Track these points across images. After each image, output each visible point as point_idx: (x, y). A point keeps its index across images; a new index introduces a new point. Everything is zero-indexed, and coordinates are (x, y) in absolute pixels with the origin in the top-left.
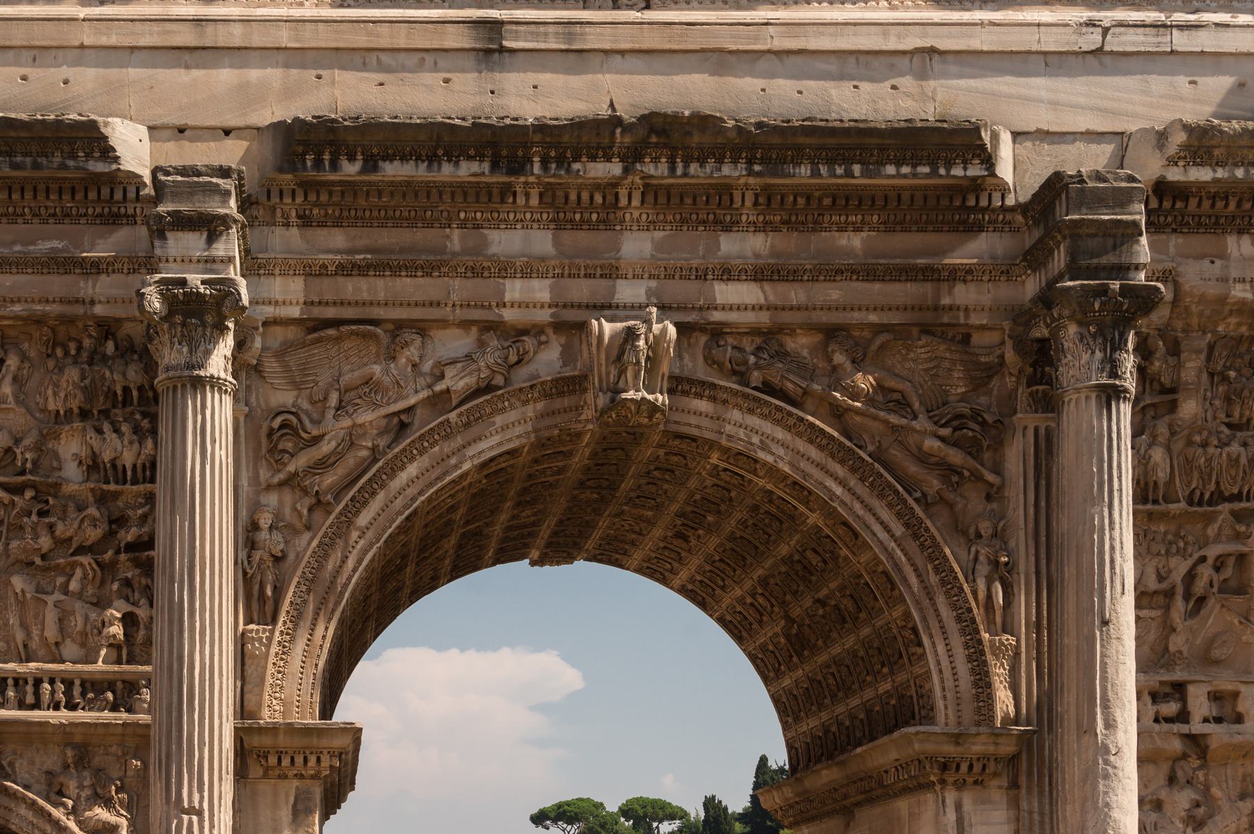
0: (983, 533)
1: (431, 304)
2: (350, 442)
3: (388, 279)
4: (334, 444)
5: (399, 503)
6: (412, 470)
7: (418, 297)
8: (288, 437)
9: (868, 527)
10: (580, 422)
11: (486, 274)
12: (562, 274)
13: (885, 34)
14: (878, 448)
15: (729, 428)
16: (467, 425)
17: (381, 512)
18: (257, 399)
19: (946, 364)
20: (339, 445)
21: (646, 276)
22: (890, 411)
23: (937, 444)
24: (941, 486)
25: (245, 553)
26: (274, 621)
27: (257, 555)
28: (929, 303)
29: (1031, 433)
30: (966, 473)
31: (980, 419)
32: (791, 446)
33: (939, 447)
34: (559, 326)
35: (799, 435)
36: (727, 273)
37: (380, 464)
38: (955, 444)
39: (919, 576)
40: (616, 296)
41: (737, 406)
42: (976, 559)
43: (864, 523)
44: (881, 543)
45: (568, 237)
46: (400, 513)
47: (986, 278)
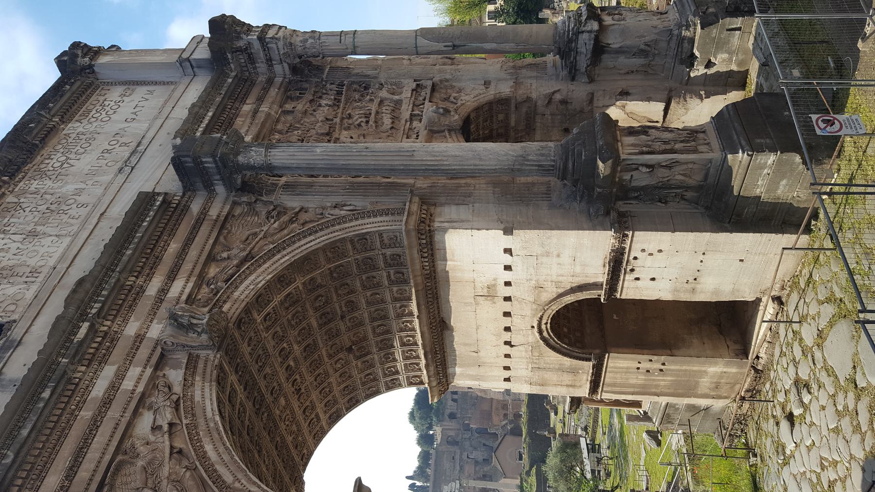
0: (321, 212)
3: (89, 451)
5: (226, 457)
6: (209, 448)
11: (112, 397)
12: (130, 360)
13: (85, 229)
15: (242, 297)
16: (193, 415)
19: (243, 222)
21: (150, 324)
34: (158, 367)
35: (255, 270)
36: (164, 291)
41: (232, 293)
42: (332, 215)
45: (112, 359)
46: (233, 456)
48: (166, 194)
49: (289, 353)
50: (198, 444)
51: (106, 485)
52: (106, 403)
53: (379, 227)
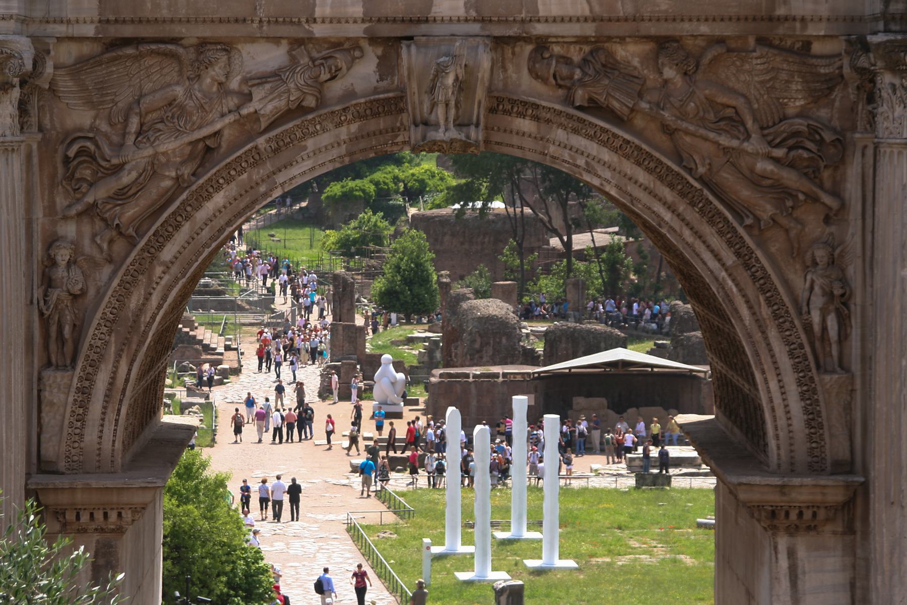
0: (818, 260)
1: (237, 21)
2: (153, 171)
4: (134, 174)
5: (205, 234)
6: (219, 199)
8: (85, 165)
9: (698, 255)
10: (397, 144)
14: (709, 170)
16: (276, 151)
17: (186, 245)
20: (140, 175)
22: (719, 131)
23: (769, 167)
24: (774, 211)
25: (41, 291)
26: (74, 360)
27: (55, 295)
28: (763, 13)
30: (801, 197)
31: (818, 137)
32: (618, 169)
35: (627, 157)
37: (184, 196)
38: (792, 165)
39: (750, 308)
40: (434, 9)
42: (812, 288)
43: (694, 251)
44: (712, 272)
46: (206, 245)
50: (221, 181)
51: (137, 48)
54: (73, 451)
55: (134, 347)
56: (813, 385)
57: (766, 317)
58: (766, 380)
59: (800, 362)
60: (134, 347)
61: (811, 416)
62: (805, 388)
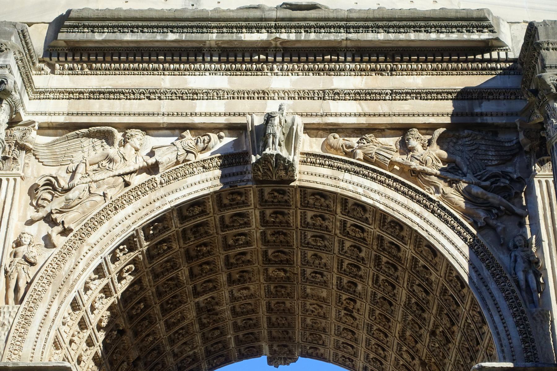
5: (118, 230)
6: (129, 209)
7: (141, 111)
8: (48, 191)
11: (185, 97)
15: (342, 184)
16: (168, 182)
17: (105, 235)
18: (32, 171)
20: (80, 193)
27: (17, 259)
28: (467, 111)
29: (544, 184)
31: (508, 177)
33: (482, 193)
38: (494, 191)
42: (516, 261)
47: (502, 97)
48: (497, 39)
49: (361, 277)
52: (176, 94)
53: (498, 334)
54: (14, 356)
55: (64, 293)
56: (524, 315)
57: (487, 276)
58: (491, 316)
59: (513, 302)
60: (64, 293)
61: (525, 335)
62: (518, 318)
